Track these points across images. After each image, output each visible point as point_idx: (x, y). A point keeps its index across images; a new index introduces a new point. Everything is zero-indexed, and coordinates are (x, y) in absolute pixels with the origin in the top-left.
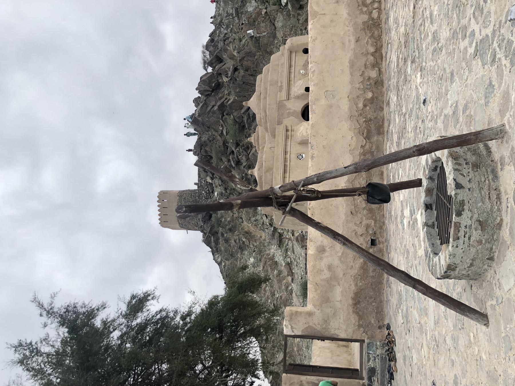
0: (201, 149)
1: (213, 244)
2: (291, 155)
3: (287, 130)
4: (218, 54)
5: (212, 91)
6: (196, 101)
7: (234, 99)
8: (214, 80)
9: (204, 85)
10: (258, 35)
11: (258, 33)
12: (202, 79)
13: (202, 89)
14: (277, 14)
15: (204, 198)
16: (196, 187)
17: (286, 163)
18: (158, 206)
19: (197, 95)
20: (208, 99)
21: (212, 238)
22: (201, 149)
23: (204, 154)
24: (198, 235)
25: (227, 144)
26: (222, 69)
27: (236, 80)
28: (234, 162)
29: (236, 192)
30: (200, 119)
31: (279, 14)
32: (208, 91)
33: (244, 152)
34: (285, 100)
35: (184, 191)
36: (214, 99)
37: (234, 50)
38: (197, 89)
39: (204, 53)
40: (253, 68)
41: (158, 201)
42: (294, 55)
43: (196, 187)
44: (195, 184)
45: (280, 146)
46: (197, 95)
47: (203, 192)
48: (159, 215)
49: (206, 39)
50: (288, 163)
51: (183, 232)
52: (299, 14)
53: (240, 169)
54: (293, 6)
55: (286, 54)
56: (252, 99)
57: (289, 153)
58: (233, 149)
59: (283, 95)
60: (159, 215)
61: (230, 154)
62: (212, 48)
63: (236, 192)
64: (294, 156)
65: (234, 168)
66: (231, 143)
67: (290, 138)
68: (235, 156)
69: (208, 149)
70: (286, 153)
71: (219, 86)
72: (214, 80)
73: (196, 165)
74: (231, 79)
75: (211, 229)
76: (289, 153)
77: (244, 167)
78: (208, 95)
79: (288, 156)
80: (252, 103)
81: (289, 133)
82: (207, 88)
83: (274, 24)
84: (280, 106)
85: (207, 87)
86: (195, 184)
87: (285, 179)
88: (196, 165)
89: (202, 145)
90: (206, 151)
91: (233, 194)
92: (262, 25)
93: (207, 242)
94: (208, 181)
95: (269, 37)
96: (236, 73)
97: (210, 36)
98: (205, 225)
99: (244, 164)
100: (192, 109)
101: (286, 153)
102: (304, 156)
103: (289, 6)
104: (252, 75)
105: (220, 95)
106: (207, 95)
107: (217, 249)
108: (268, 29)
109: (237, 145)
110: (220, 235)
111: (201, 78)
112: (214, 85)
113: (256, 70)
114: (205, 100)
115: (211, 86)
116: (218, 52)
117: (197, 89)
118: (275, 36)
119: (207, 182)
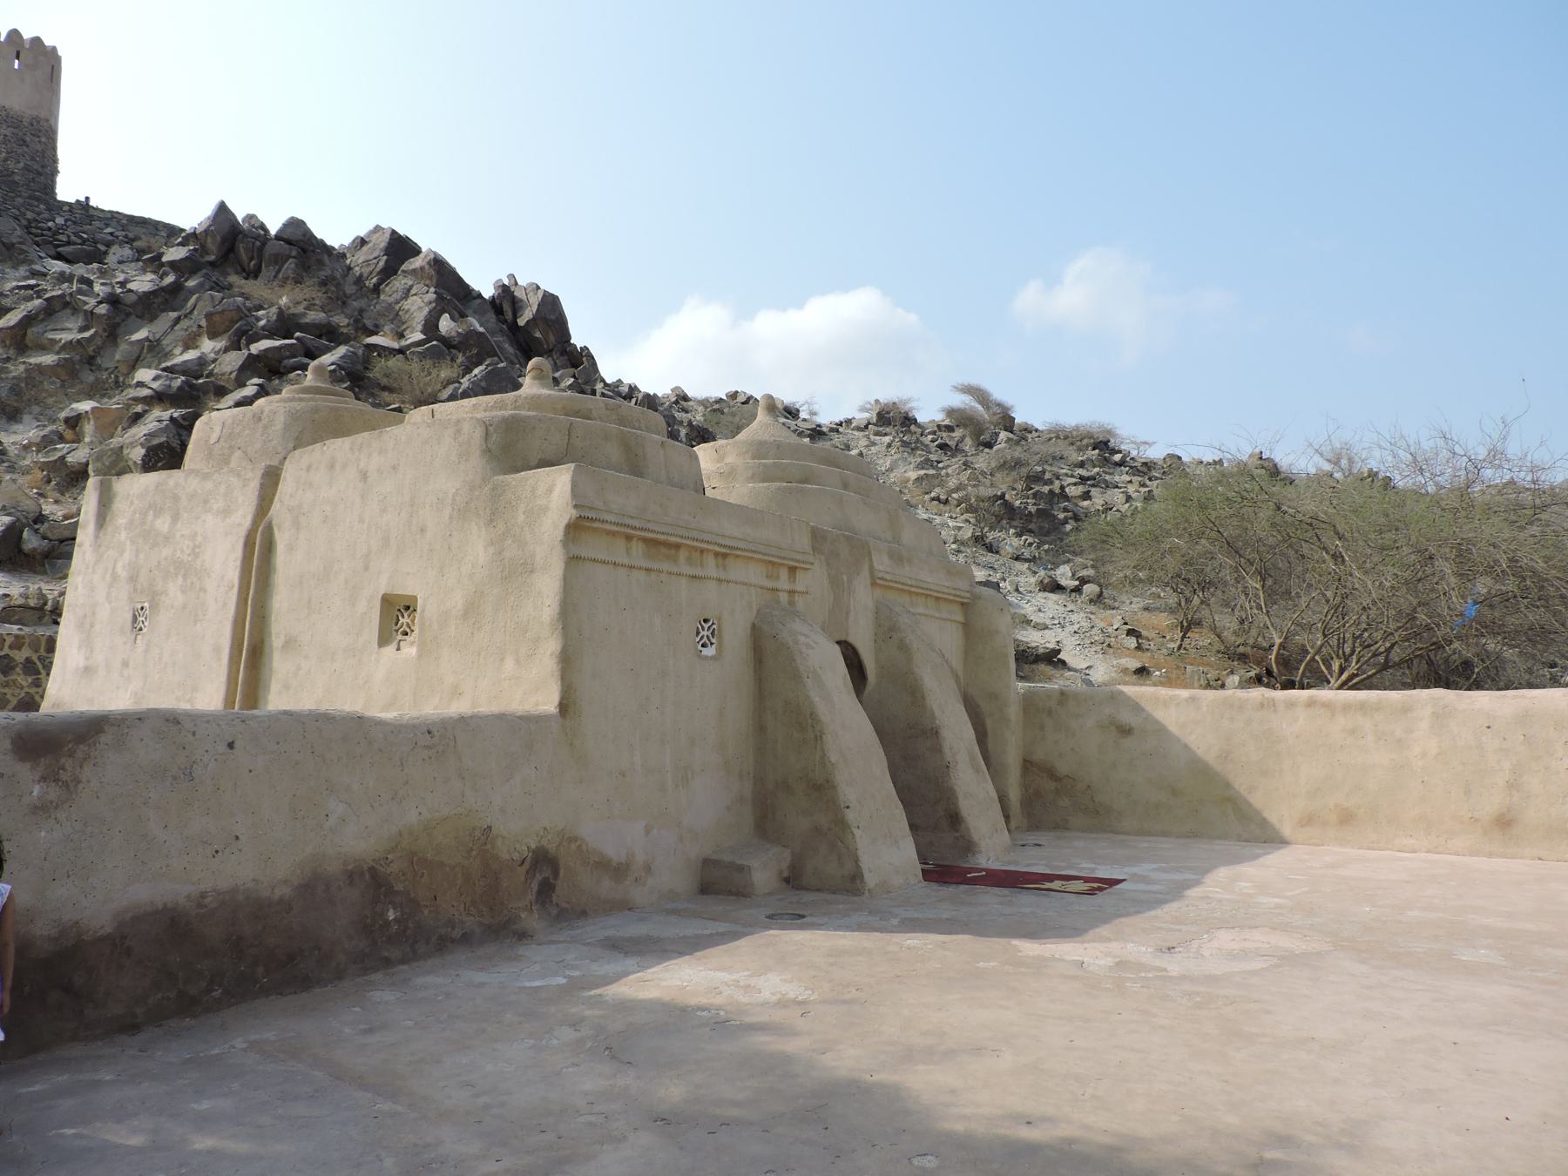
0: (289, 242)
15: (30, 215)
17: (683, 554)
22: (289, 242)
34: (871, 568)
38: (511, 276)
47: (60, 220)
67: (770, 584)
69: (290, 265)
79: (711, 568)
87: (621, 543)
89: (304, 251)
90: (279, 260)
94: (115, 248)
102: (710, 651)
112: (538, 335)
117: (511, 276)
119: (108, 245)
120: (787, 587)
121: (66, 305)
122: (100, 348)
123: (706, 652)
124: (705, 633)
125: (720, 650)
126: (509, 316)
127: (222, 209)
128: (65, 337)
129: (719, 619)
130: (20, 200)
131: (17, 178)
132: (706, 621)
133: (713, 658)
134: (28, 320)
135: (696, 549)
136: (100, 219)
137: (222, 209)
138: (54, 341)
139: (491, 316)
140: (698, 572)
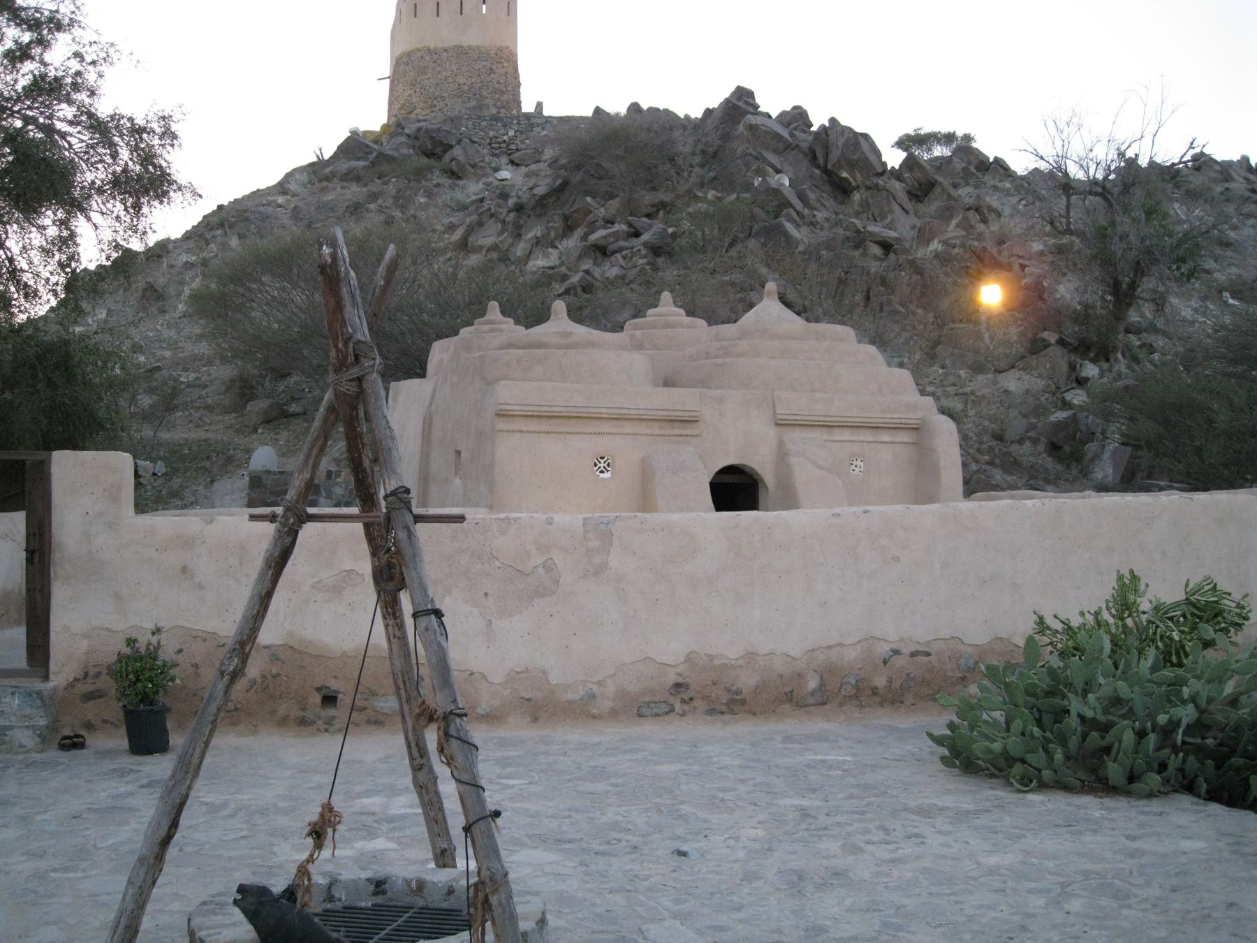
1: (344, 166)
4: (938, 190)
5: (825, 171)
6: (798, 117)
7: (797, 243)
8: (858, 175)
9: (845, 145)
12: (862, 141)
13: (832, 137)
14: (1040, 376)
15: (492, 134)
16: (528, 107)
19: (818, 120)
20: (801, 156)
21: (362, 163)
24: (373, 116)
25: (661, 213)
26: (889, 204)
27: (857, 247)
28: (605, 237)
29: (510, 240)
30: (741, 128)
31: (1041, 383)
32: (827, 155)
33: (635, 271)
35: (516, 69)
37: (944, 242)
38: (833, 121)
39: (949, 138)
40: (890, 302)
43: (528, 107)
44: (539, 106)
46: (818, 120)
47: (511, 133)
49: (989, 147)
51: (384, 66)
52: (1035, 441)
53: (581, 257)
54: (1059, 425)
55: (912, 417)
58: (645, 237)
61: (630, 225)
62: (959, 165)
63: (510, 240)
65: (584, 238)
66: (665, 230)
68: (623, 243)
71: (842, 190)
72: (858, 175)
73: (598, 111)
74: (858, 231)
75: (393, 158)
77: (587, 272)
78: (815, 157)
80: (768, 310)
82: (835, 155)
83: (1013, 367)
85: (839, 152)
86: (539, 106)
88: (598, 111)
91: (502, 232)
93: (354, 145)
95: (977, 352)
96: (876, 250)
97: (996, 159)
98: (403, 139)
99: (597, 272)
100: (772, 102)
103: (1061, 415)
104: (868, 298)
105: (812, 196)
107: (327, 179)
108: (1001, 350)
109: (655, 251)
110: (376, 186)
111: (865, 136)
112: (845, 175)
113: (881, 310)
114: (797, 146)
115: (841, 167)
116: (944, 190)
117: (833, 121)
118: (978, 369)
121: (492, 215)
122: (512, 245)
123: (602, 475)
128: (488, 241)
130: (484, 124)
131: (487, 101)
134: (470, 231)
136: (538, 125)
138: (481, 247)
139: (805, 164)
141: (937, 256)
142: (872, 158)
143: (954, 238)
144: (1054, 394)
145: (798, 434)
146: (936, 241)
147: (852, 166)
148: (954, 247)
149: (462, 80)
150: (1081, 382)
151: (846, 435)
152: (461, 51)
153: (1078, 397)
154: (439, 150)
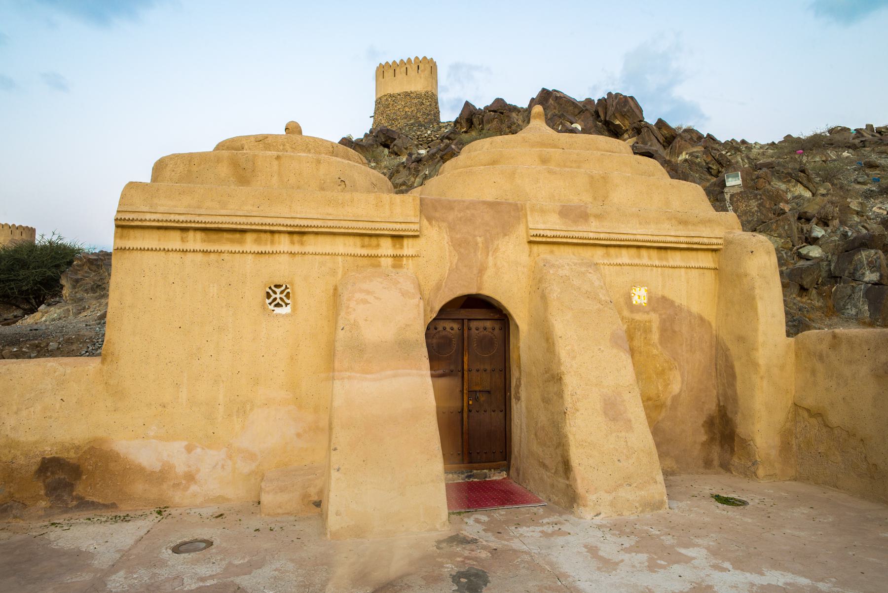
0: (495, 111)
2: (285, 258)
3: (397, 238)
9: (617, 103)
10: (727, 197)
11: (732, 196)
12: (630, 100)
14: (780, 236)
15: (419, 133)
17: (249, 237)
18: (409, 60)
22: (495, 111)
23: (485, 119)
26: (649, 136)
35: (437, 103)
36: (589, 125)
37: (691, 154)
41: (417, 58)
42: (707, 260)
45: (330, 210)
47: (429, 132)
48: (394, 62)
50: (250, 244)
56: (548, 128)
57: (296, 248)
59: (549, 224)
60: (394, 62)
64: (279, 268)
67: (365, 252)
70: (299, 233)
76: (296, 248)
78: (598, 116)
79: (284, 244)
81: (386, 247)
82: (611, 110)
84: (506, 213)
87: (177, 234)
92: (754, 204)
101: (299, 233)
106: (597, 113)
111: (632, 98)
112: (617, 122)
120: (391, 252)
123: (278, 310)
124: (278, 296)
125: (294, 309)
126: (602, 117)
127: (467, 104)
129: (292, 284)
132: (277, 286)
133: (286, 315)
135: (265, 231)
137: (467, 104)
140: (268, 248)
141: (686, 160)
142: (637, 111)
143: (697, 152)
144: (791, 250)
145: (566, 257)
146: (684, 153)
147: (623, 116)
148: (697, 157)
149: (407, 109)
150: (814, 241)
151: (625, 256)
152: (407, 94)
153: (815, 252)
154: (388, 142)
